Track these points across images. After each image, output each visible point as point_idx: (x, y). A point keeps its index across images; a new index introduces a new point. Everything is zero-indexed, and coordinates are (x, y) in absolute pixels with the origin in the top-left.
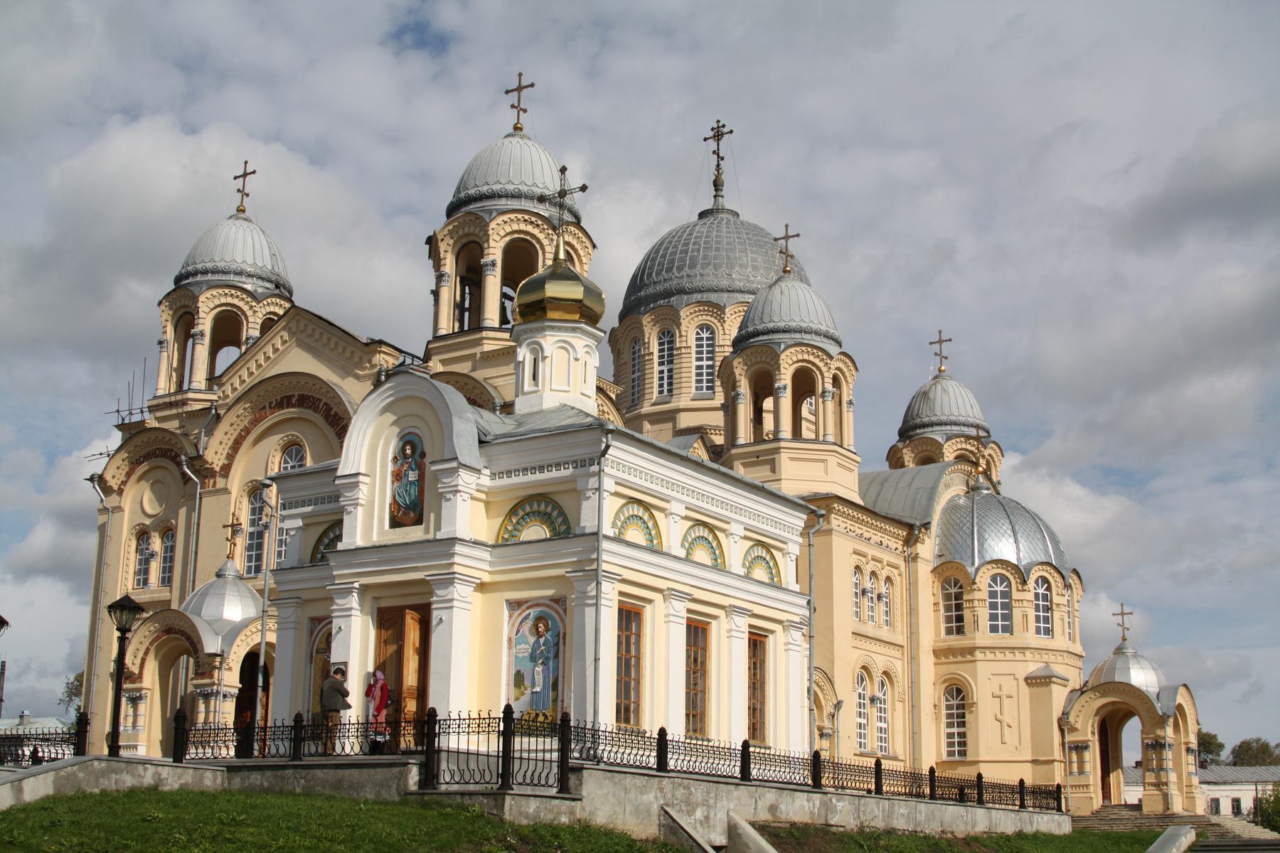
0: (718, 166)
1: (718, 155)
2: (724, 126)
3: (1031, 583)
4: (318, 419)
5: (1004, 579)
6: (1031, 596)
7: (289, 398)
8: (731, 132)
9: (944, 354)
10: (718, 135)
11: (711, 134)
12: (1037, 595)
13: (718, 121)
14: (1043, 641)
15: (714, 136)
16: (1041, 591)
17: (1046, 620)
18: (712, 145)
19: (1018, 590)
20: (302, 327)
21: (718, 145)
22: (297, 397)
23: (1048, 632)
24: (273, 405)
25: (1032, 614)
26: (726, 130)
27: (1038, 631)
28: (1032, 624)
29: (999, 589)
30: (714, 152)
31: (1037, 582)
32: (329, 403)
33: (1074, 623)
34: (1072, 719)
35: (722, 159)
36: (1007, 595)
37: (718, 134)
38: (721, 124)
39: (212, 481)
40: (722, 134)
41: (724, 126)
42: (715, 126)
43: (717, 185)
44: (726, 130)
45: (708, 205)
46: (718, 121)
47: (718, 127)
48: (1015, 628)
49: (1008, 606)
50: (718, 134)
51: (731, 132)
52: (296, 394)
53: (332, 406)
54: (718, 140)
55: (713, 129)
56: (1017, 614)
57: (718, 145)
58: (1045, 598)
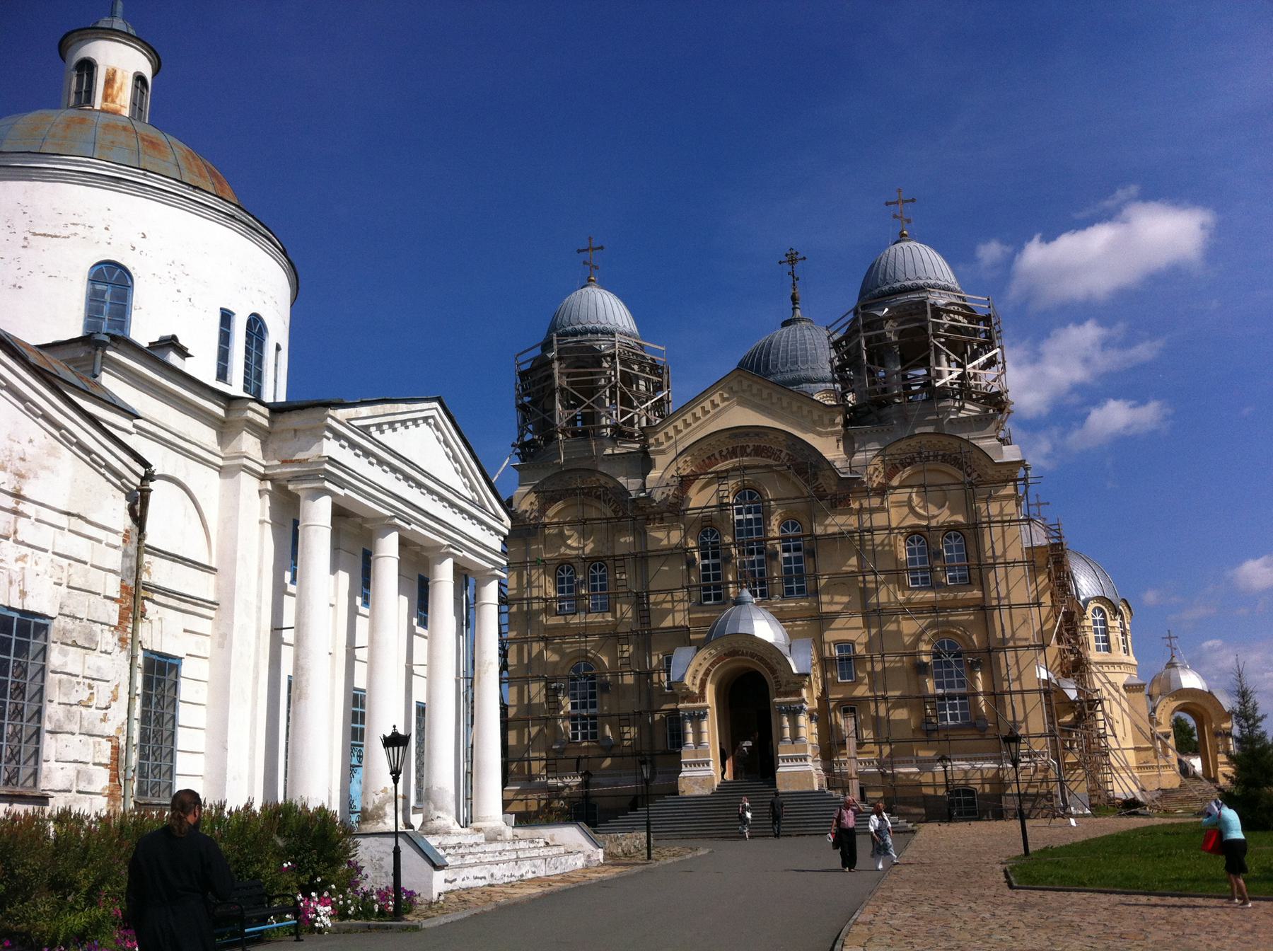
1: (794, 277)
2: (797, 253)
5: (1101, 610)
7: (743, 449)
8: (804, 258)
10: (792, 261)
11: (787, 259)
13: (791, 249)
16: (1098, 618)
19: (1111, 619)
20: (745, 387)
22: (751, 448)
24: (724, 453)
26: (799, 256)
29: (1098, 618)
34: (1157, 715)
35: (798, 279)
36: (1104, 623)
41: (797, 253)
44: (799, 256)
48: (1113, 648)
49: (1106, 631)
50: (792, 259)
52: (751, 445)
55: (787, 255)
56: (1112, 636)
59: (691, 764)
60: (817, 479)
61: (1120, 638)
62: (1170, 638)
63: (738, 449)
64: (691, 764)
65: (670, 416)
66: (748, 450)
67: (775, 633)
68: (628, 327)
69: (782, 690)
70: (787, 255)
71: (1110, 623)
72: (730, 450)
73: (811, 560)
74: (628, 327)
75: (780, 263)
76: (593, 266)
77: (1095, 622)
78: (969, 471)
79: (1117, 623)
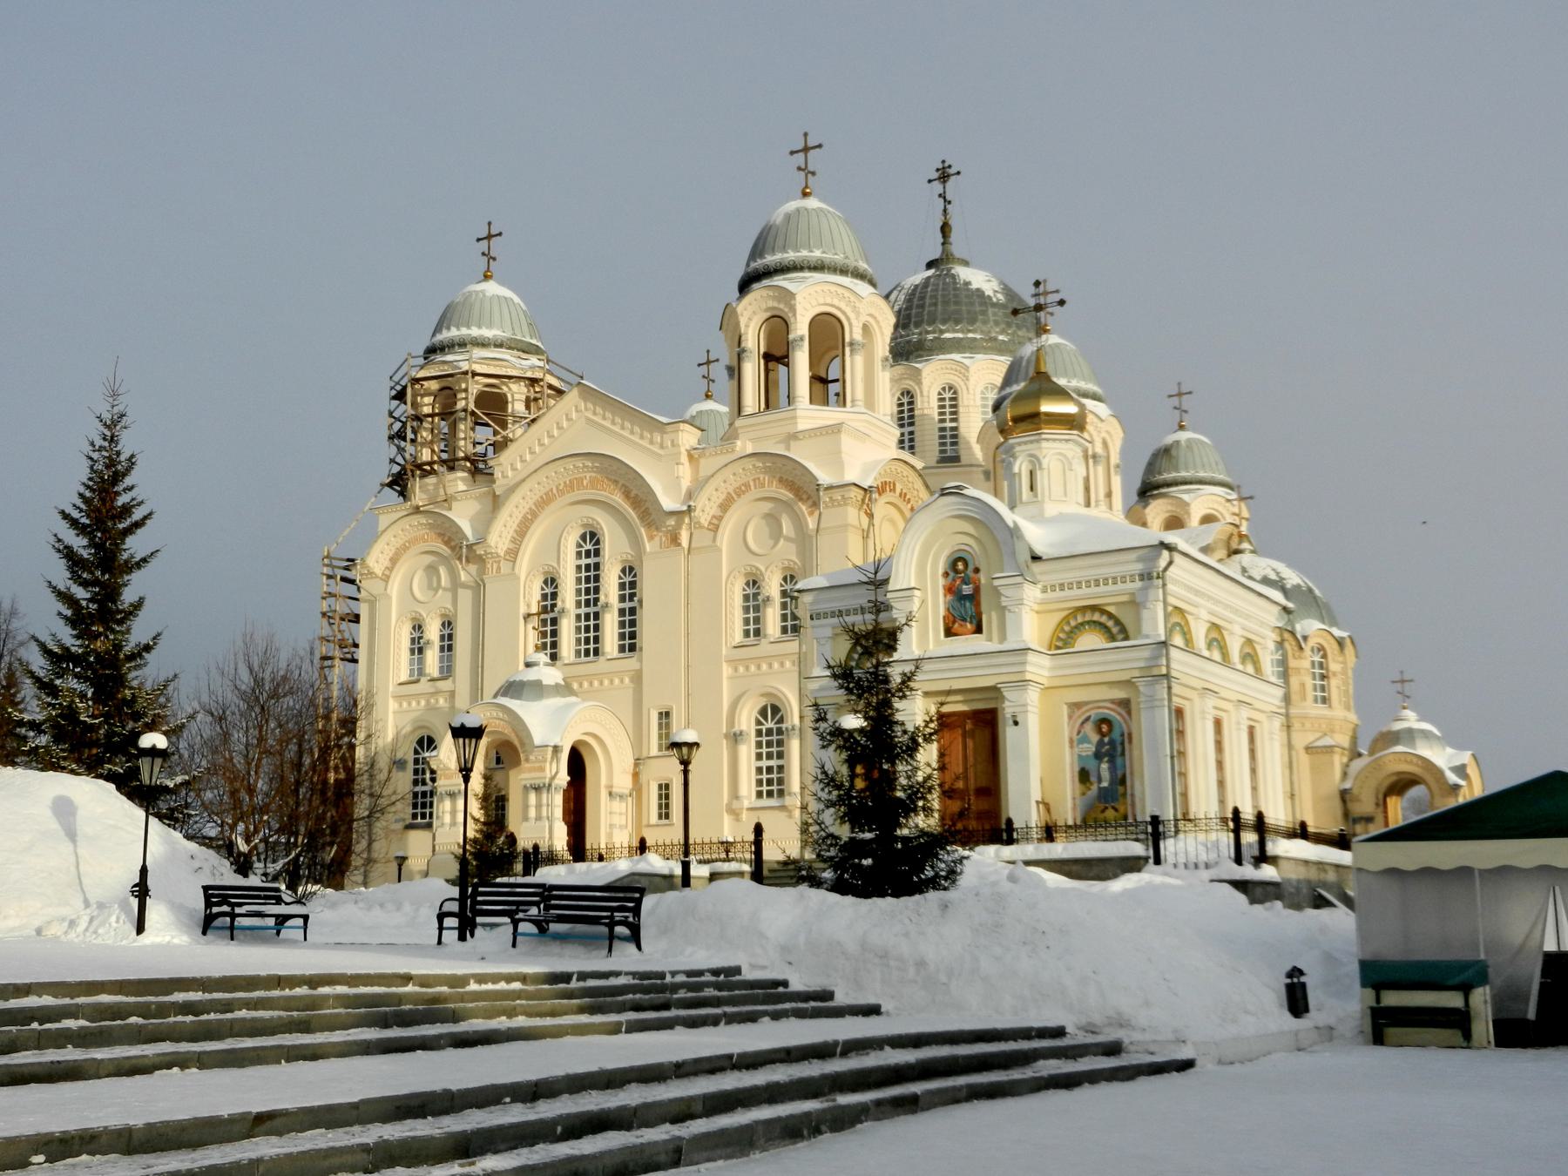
0: (945, 210)
1: (945, 200)
2: (950, 167)
3: (1307, 651)
6: (1306, 664)
8: (958, 173)
9: (1184, 408)
11: (936, 175)
12: (1313, 662)
13: (943, 162)
14: (1321, 710)
15: (940, 178)
17: (1323, 689)
18: (938, 187)
23: (1324, 700)
25: (1309, 682)
26: (952, 171)
27: (1316, 701)
28: (1310, 694)
32: (628, 484)
35: (950, 202)
37: (944, 175)
38: (946, 165)
40: (948, 176)
41: (950, 167)
42: (940, 166)
43: (945, 229)
44: (952, 171)
45: (936, 253)
46: (943, 162)
50: (944, 175)
51: (958, 173)
54: (944, 182)
58: (1321, 666)
60: (650, 514)
75: (930, 181)
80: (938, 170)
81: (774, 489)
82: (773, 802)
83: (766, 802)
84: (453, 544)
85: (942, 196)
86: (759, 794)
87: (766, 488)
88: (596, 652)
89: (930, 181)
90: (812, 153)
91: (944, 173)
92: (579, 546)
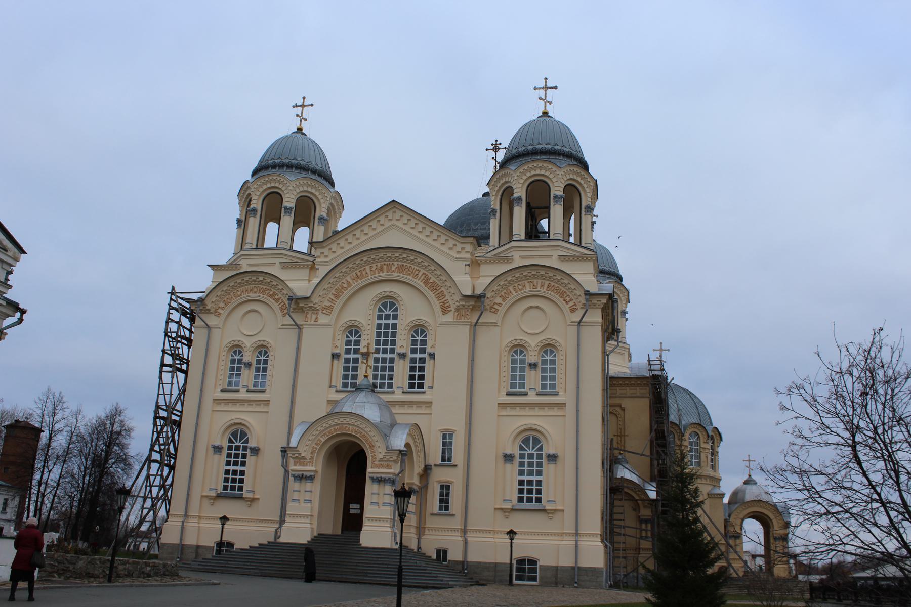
1: (496, 160)
2: (500, 144)
4: (419, 283)
10: (496, 149)
11: (491, 147)
13: (496, 141)
15: (493, 149)
21: (496, 154)
22: (396, 266)
26: (501, 146)
30: (493, 158)
31: (691, 435)
32: (427, 273)
33: (715, 459)
34: (732, 519)
36: (698, 444)
38: (498, 143)
39: (314, 316)
40: (499, 149)
41: (500, 144)
42: (495, 143)
44: (501, 146)
46: (496, 141)
47: (496, 144)
48: (703, 464)
53: (430, 276)
54: (496, 151)
56: (703, 456)
57: (496, 154)
59: (293, 516)
61: (710, 457)
62: (749, 461)
63: (385, 266)
64: (293, 516)
65: (336, 233)
66: (393, 268)
67: (381, 416)
68: (320, 165)
69: (377, 463)
70: (492, 145)
71: (703, 445)
72: (379, 266)
73: (432, 362)
74: (320, 165)
75: (487, 150)
76: (303, 118)
77: (691, 443)
78: (568, 299)
79: (708, 446)
80: (492, 145)
81: (545, 290)
82: (534, 505)
83: (525, 505)
84: (276, 297)
85: (495, 159)
86: (521, 500)
87: (538, 289)
88: (390, 386)
89: (487, 150)
90: (549, 91)
91: (496, 146)
92: (380, 310)
